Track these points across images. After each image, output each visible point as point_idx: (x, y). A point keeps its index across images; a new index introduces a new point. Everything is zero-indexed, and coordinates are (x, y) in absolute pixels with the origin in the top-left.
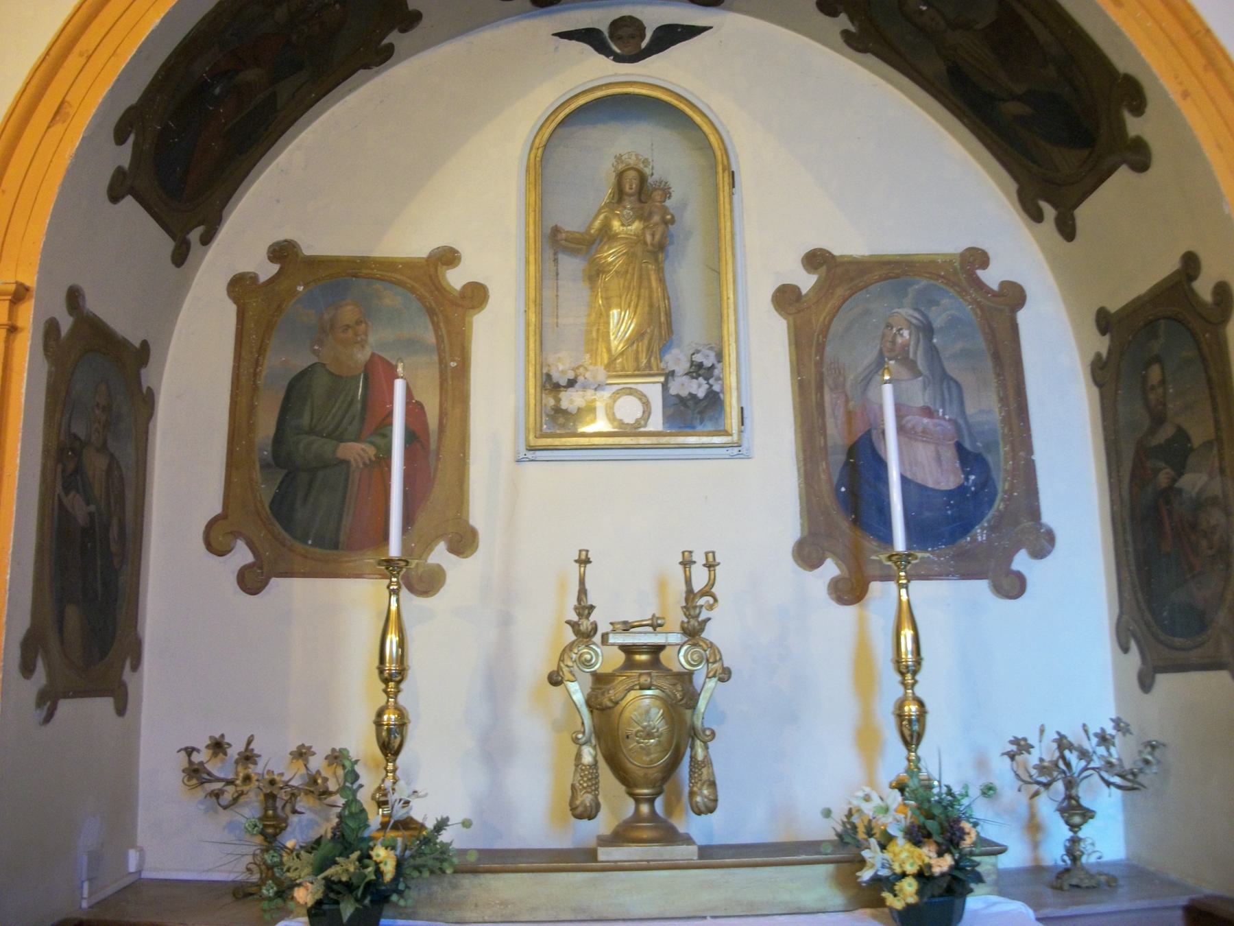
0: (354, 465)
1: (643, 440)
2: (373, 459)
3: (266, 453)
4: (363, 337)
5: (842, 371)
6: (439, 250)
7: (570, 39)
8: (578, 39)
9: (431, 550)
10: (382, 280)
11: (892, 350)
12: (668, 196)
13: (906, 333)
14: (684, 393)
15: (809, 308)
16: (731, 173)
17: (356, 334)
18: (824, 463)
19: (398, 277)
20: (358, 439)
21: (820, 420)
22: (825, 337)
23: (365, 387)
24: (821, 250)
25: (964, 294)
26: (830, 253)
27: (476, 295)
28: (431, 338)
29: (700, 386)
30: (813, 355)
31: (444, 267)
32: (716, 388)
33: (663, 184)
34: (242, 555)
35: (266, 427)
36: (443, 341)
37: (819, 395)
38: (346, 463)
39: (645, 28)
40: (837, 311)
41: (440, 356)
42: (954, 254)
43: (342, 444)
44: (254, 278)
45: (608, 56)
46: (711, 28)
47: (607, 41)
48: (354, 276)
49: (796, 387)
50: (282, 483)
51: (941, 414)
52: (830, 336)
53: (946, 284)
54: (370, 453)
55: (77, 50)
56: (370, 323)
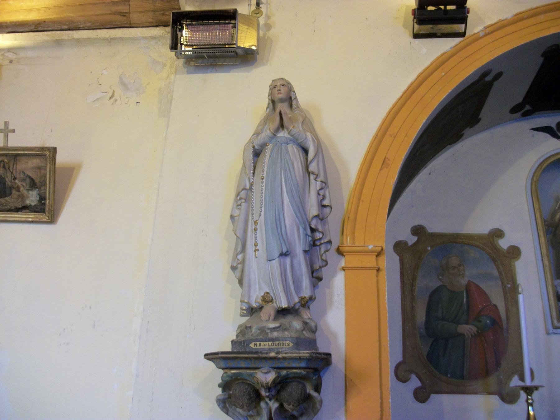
0: (467, 336)
2: (476, 333)
3: (422, 330)
4: (463, 272)
9: (511, 380)
10: (468, 244)
20: (467, 323)
23: (467, 297)
27: (515, 252)
28: (496, 273)
31: (497, 238)
34: (415, 382)
35: (421, 317)
38: (461, 335)
41: (502, 282)
43: (460, 326)
44: (406, 243)
50: (432, 345)
54: (473, 330)
55: (388, 133)
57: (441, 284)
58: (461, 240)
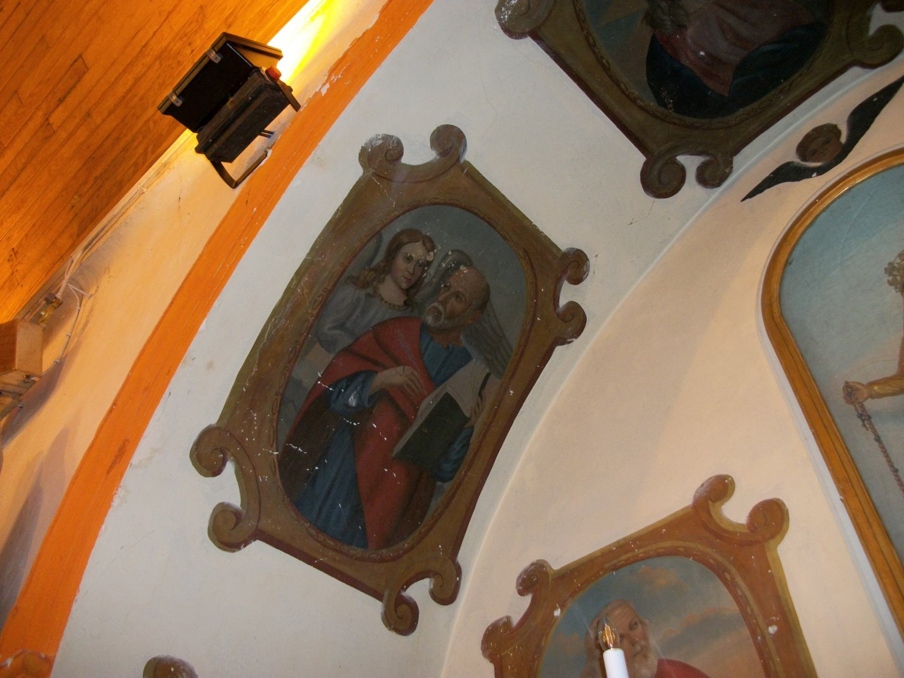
4: (643, 643)
6: (705, 486)
7: (761, 191)
8: (769, 187)
19: (668, 544)
28: (727, 603)
31: (717, 504)
36: (748, 603)
44: (506, 623)
45: (810, 177)
47: (802, 165)
48: (614, 570)
56: (647, 621)
58: (629, 555)
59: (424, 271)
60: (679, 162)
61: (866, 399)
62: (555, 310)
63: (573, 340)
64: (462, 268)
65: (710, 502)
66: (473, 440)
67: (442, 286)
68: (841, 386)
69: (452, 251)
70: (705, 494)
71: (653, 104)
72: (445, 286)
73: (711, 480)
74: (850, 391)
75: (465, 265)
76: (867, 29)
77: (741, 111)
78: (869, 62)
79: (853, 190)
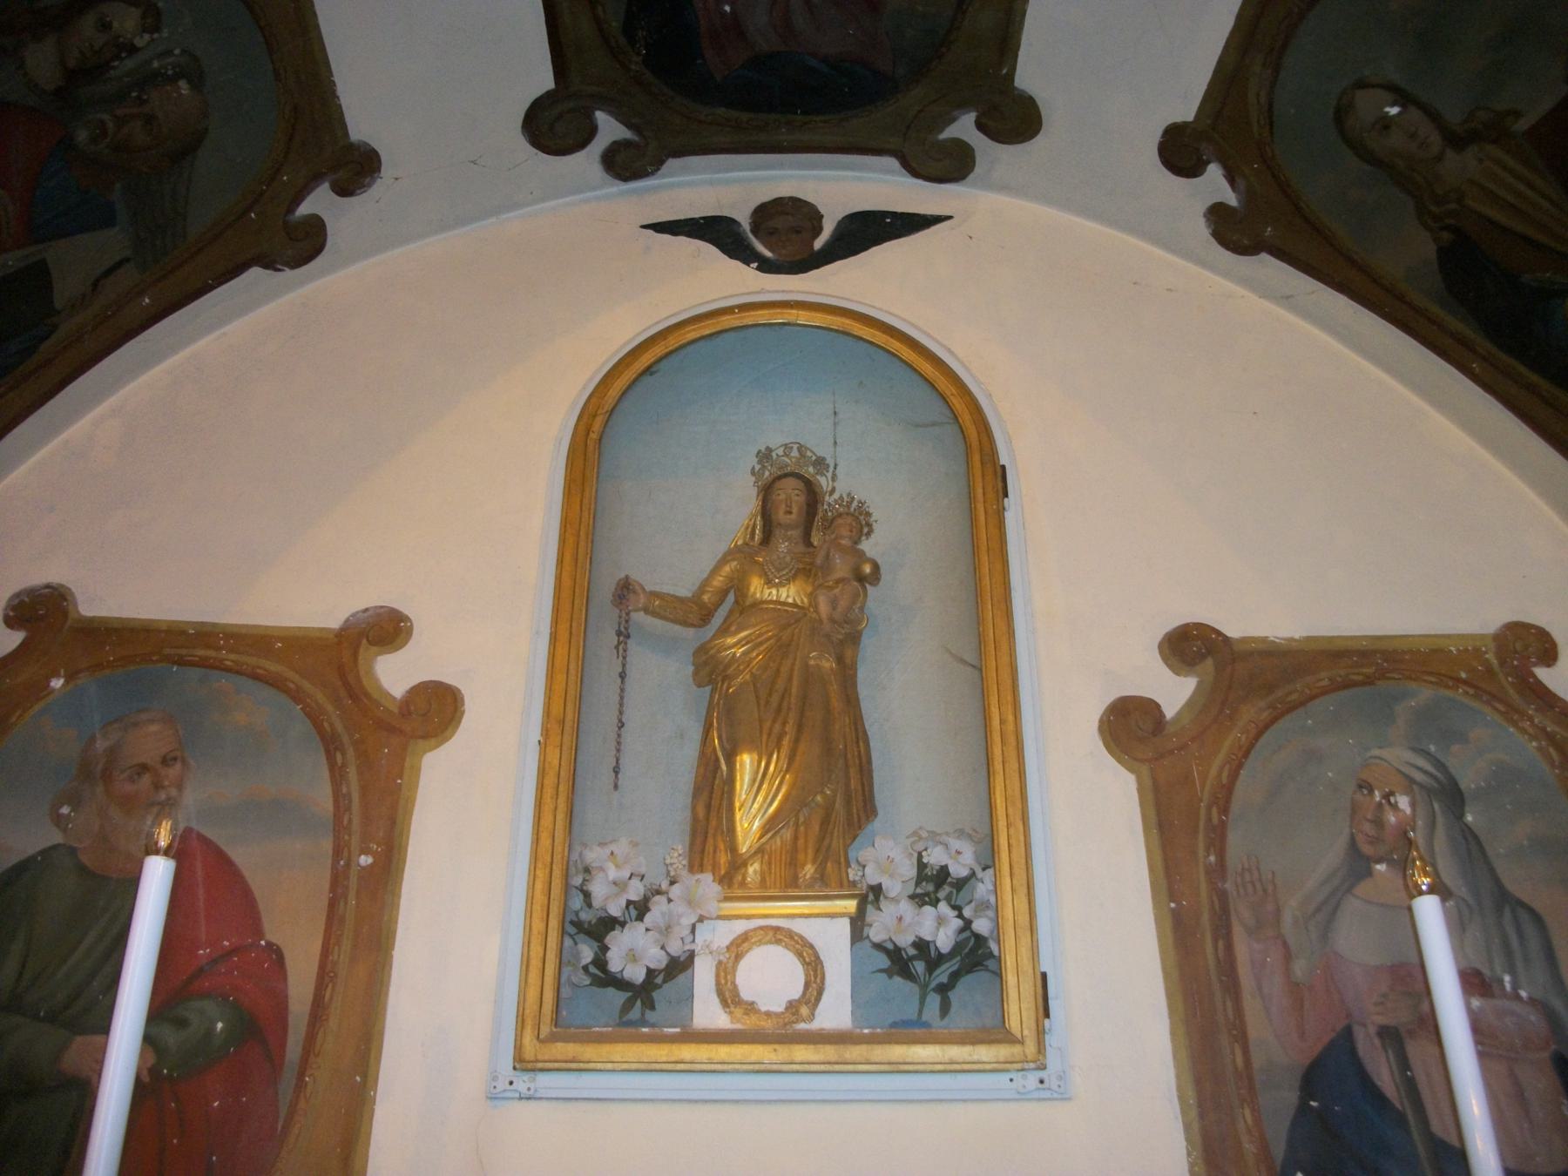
1: (802, 1053)
4: (173, 792)
5: (1270, 889)
7: (675, 234)
8: (690, 235)
11: (1374, 841)
12: (866, 530)
13: (1403, 802)
14: (905, 940)
15: (1183, 747)
16: (999, 470)
17: (158, 786)
18: (1247, 1112)
19: (273, 667)
21: (1229, 1004)
22: (1225, 810)
24: (1199, 626)
25: (1515, 717)
26: (1219, 633)
28: (321, 796)
29: (941, 921)
30: (1201, 852)
31: (375, 649)
32: (982, 926)
33: (855, 504)
36: (349, 809)
37: (1221, 944)
39: (822, 216)
40: (1246, 754)
42: (1483, 637)
43: (79, 1039)
45: (747, 262)
46: (950, 218)
47: (747, 238)
48: (175, 663)
49: (1168, 924)
51: (1508, 987)
52: (1235, 807)
53: (1476, 697)
56: (192, 762)
57: (57, 838)
58: (211, 653)
59: (117, 57)
60: (596, 119)
61: (637, 610)
62: (286, 215)
63: (285, 268)
64: (183, 84)
65: (364, 641)
66: (44, 346)
67: (134, 94)
68: (622, 575)
69: (184, 51)
70: (364, 626)
71: (615, 25)
72: (139, 97)
73: (382, 610)
74: (625, 590)
75: (189, 82)
76: (941, 131)
77: (721, 111)
78: (914, 165)
79: (787, 327)
